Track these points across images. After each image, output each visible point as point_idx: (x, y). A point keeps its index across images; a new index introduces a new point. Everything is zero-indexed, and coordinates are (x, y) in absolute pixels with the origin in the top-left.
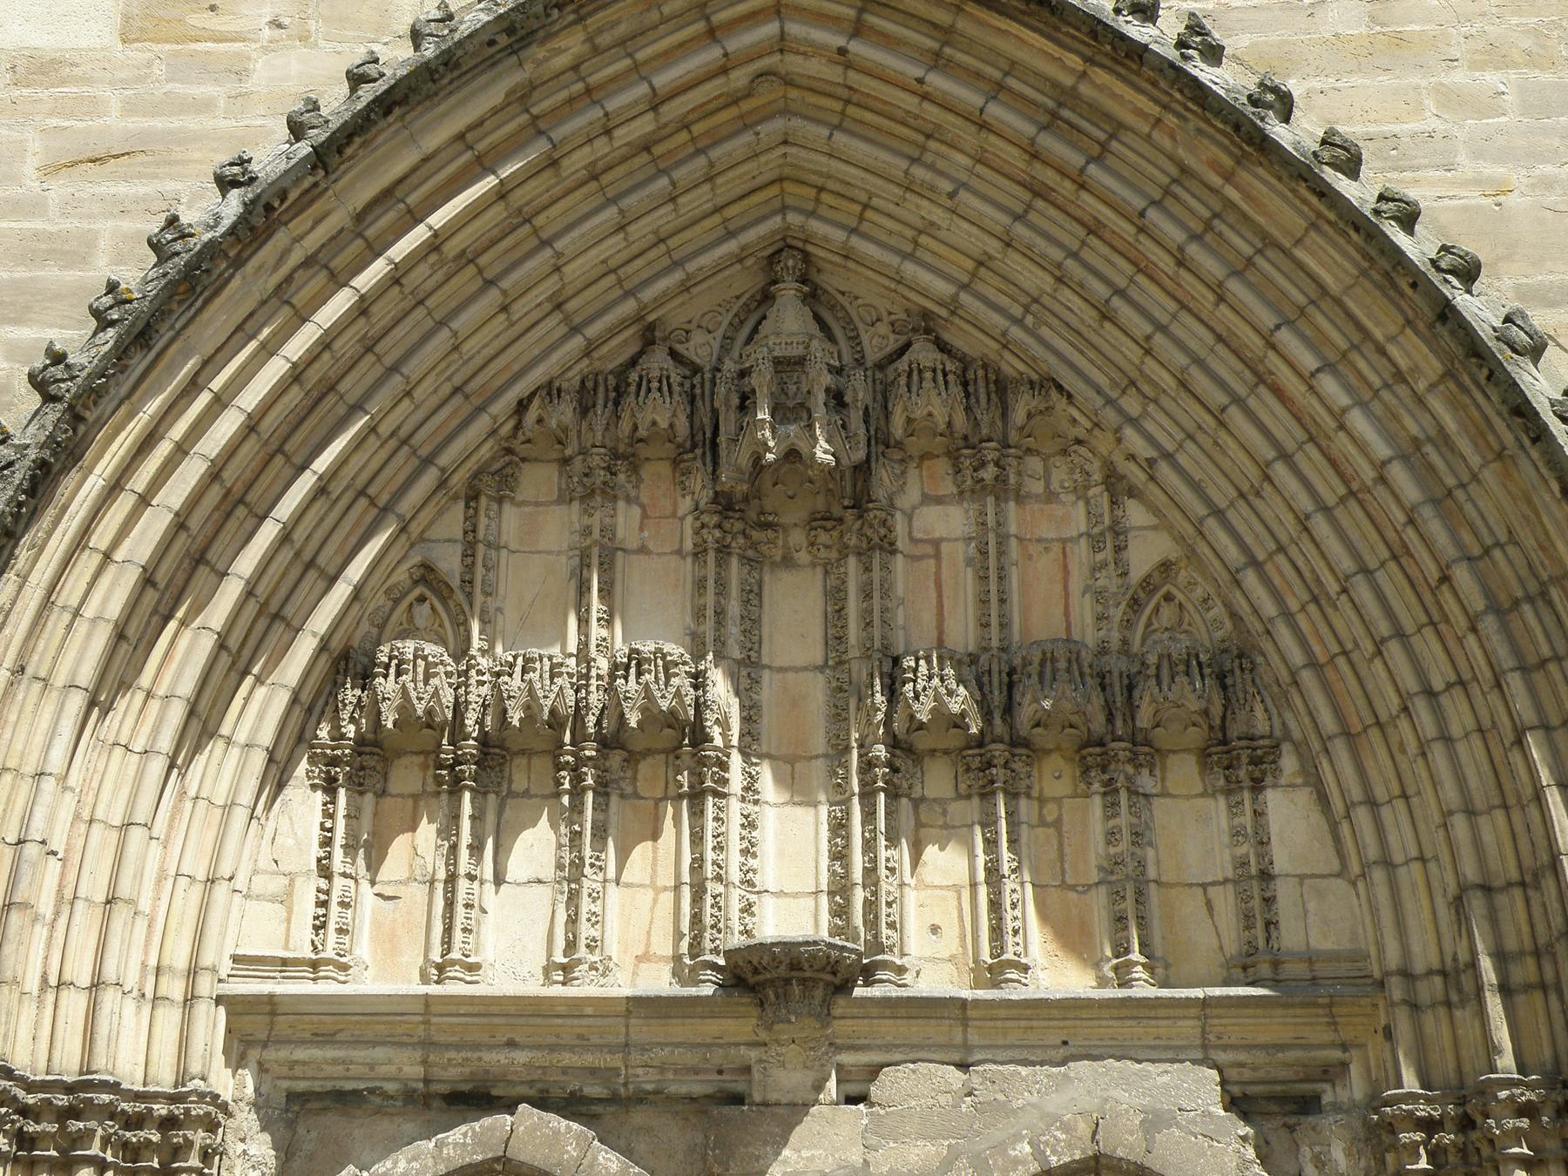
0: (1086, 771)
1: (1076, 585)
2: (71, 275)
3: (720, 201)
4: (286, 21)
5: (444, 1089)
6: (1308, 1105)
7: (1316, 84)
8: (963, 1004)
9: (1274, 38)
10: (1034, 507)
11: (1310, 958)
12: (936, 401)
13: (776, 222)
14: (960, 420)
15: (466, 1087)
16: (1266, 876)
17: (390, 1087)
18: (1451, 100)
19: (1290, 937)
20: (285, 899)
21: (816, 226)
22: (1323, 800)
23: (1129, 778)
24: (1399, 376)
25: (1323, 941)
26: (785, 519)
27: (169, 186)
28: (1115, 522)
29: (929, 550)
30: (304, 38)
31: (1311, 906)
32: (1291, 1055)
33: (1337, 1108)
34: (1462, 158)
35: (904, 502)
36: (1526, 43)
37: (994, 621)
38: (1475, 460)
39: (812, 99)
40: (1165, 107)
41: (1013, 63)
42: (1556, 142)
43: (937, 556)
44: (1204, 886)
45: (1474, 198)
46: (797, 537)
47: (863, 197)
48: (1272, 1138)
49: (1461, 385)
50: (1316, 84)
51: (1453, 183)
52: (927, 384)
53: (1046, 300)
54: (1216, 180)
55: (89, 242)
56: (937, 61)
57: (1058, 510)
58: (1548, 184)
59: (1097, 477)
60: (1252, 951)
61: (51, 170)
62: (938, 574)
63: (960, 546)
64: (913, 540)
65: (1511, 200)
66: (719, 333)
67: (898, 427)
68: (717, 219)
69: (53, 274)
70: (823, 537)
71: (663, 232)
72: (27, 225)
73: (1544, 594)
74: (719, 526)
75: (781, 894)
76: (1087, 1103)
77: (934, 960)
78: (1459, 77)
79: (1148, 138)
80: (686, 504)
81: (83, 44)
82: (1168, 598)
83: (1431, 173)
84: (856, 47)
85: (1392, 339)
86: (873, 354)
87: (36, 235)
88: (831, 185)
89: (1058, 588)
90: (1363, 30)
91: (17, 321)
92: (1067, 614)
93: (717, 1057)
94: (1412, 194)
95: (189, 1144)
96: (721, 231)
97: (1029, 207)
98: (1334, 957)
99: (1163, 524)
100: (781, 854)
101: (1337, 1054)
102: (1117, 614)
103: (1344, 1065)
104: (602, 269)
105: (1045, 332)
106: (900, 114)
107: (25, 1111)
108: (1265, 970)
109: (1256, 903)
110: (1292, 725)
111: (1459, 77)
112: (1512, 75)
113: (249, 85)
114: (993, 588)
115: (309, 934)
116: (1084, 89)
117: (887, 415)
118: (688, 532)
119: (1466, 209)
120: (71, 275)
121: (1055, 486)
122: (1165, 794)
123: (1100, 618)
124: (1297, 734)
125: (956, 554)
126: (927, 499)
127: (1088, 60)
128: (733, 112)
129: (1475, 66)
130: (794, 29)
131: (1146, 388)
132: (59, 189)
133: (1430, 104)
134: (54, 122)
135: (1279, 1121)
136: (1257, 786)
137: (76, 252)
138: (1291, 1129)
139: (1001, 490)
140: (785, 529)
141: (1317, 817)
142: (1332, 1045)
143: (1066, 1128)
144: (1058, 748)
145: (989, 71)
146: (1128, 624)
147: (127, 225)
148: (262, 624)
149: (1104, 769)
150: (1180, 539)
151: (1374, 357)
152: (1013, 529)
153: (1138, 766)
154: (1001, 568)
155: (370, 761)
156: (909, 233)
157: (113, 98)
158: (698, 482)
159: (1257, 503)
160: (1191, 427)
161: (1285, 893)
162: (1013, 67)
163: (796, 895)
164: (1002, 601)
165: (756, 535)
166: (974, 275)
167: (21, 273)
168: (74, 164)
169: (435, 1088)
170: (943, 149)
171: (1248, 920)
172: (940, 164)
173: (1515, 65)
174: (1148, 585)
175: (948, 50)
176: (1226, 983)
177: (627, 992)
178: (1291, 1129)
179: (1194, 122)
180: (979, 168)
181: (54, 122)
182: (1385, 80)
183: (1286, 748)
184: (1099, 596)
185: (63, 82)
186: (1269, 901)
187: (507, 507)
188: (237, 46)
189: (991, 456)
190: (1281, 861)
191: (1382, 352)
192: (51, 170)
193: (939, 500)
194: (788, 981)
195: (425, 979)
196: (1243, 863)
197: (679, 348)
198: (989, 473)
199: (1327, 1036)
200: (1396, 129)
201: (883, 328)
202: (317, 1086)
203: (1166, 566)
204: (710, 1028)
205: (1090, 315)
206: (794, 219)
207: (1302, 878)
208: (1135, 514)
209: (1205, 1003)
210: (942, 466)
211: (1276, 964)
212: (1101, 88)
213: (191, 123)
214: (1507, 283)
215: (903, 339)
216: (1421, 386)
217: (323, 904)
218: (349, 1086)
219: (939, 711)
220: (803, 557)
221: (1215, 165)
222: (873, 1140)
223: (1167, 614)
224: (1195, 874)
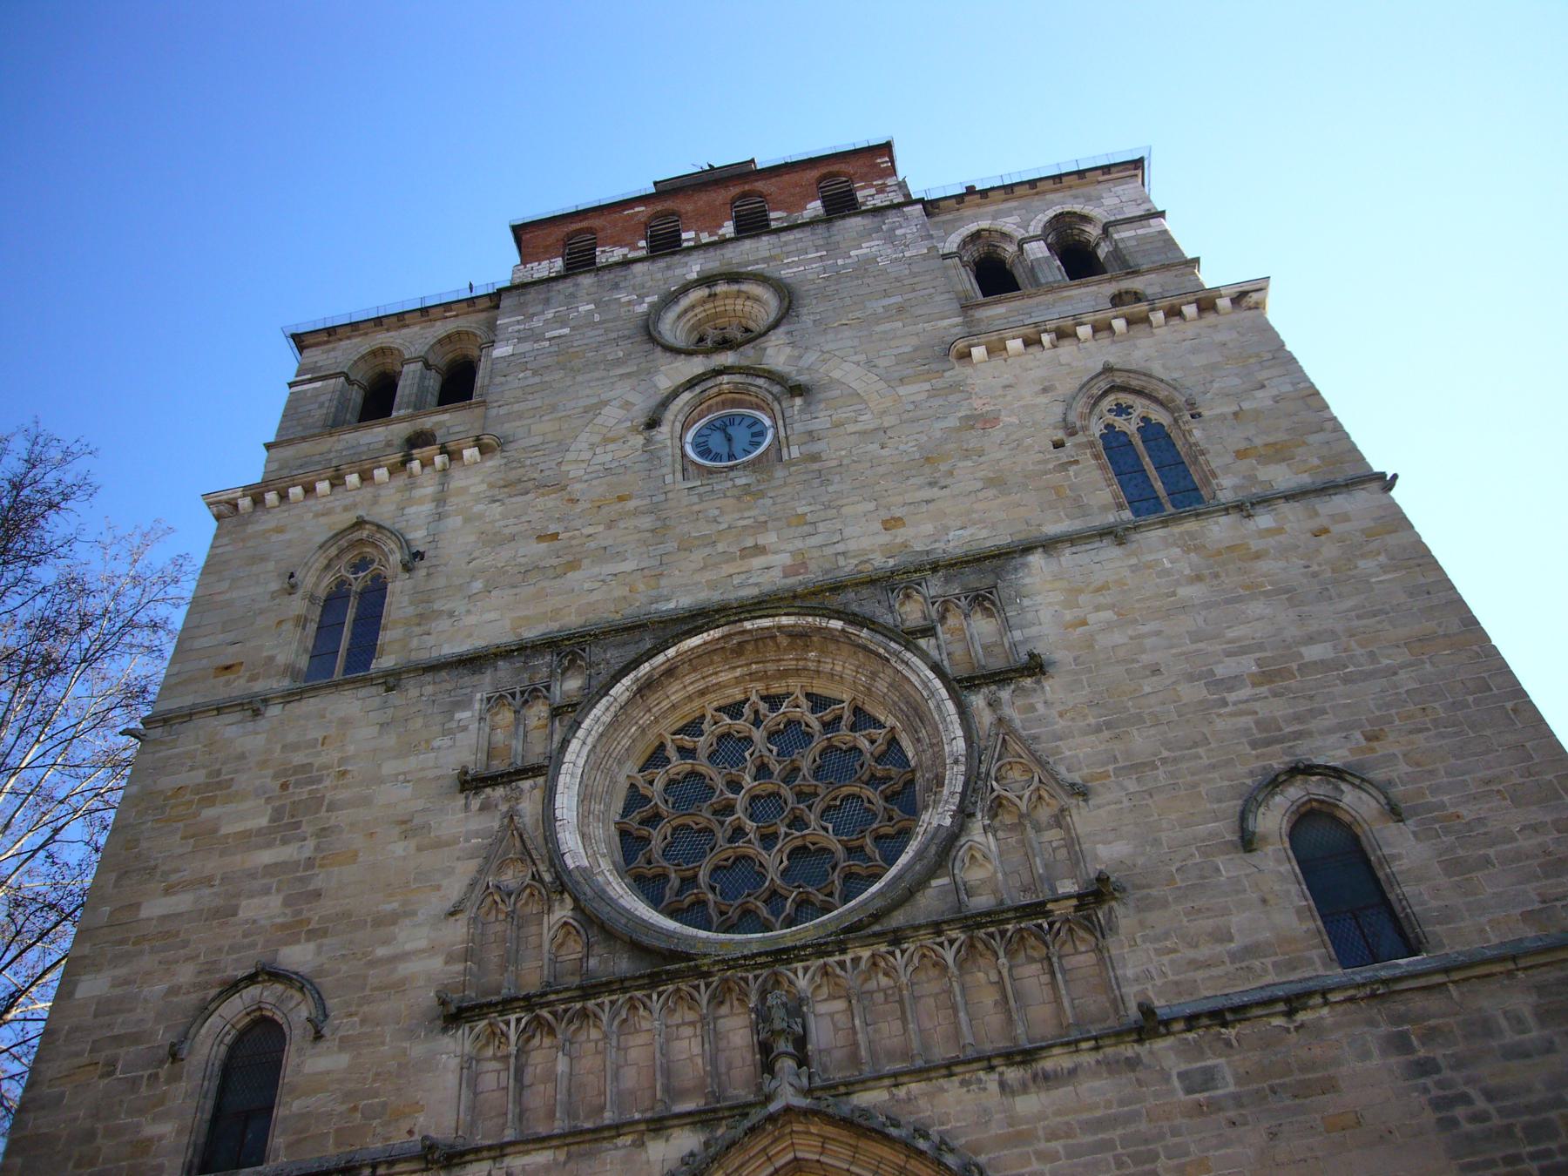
50: (992, 1155)
111: (1043, 1145)
129: (1048, 1140)
182: (1015, 1150)
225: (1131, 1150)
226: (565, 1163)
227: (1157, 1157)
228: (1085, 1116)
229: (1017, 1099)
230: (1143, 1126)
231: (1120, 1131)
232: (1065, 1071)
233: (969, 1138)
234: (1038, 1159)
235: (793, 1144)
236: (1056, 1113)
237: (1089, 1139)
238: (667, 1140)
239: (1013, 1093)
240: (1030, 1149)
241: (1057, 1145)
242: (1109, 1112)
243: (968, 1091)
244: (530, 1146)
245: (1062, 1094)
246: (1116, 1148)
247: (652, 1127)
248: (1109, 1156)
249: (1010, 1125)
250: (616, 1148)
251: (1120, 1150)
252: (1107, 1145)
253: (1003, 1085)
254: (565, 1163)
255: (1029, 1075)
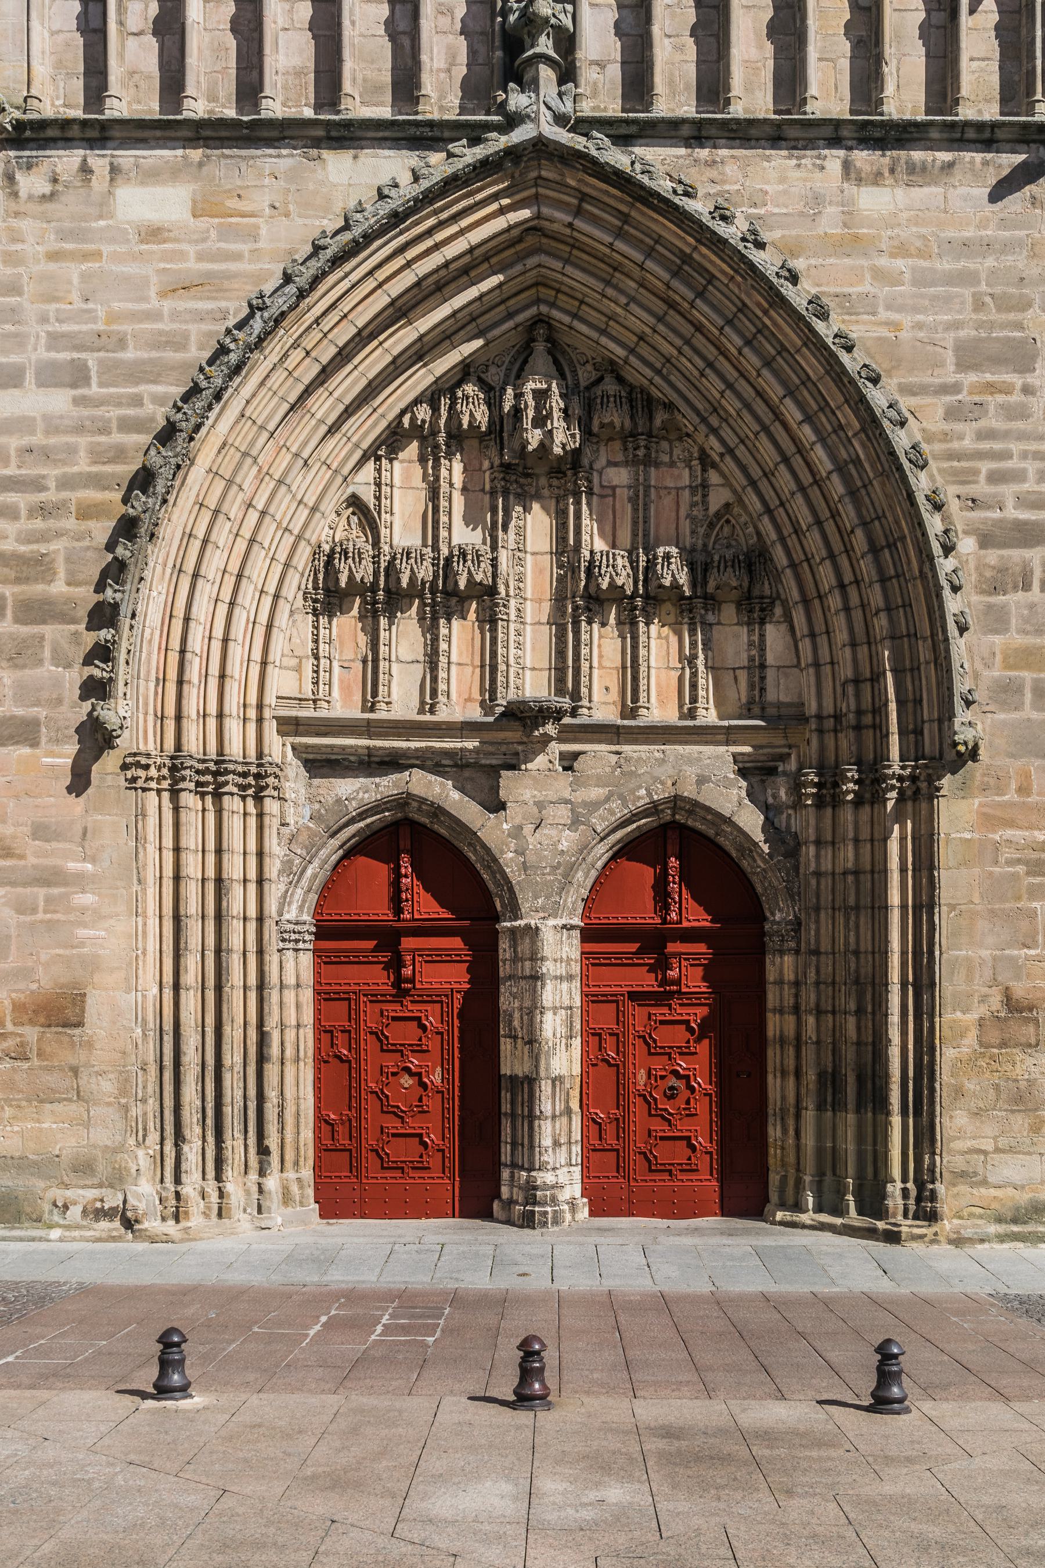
0: (682, 612)
1: (683, 513)
2: (179, 356)
3: (504, 296)
4: (277, 205)
5: (377, 759)
6: (772, 771)
7: (813, 262)
8: (618, 727)
9: (794, 233)
10: (664, 469)
11: (779, 705)
12: (616, 415)
13: (533, 311)
14: (628, 423)
15: (387, 759)
16: (763, 666)
17: (352, 758)
18: (880, 275)
19: (771, 696)
20: (298, 669)
21: (556, 314)
22: (792, 629)
23: (702, 616)
24: (841, 427)
25: (783, 698)
26: (537, 471)
27: (223, 304)
28: (704, 480)
29: (610, 492)
30: (287, 215)
31: (782, 681)
32: (766, 751)
33: (785, 773)
34: (881, 310)
35: (597, 466)
36: (919, 244)
37: (641, 520)
38: (871, 475)
39: (554, 244)
40: (736, 271)
41: (660, 236)
42: (927, 302)
43: (614, 495)
44: (734, 669)
45: (884, 332)
46: (543, 481)
47: (580, 296)
48: (755, 785)
49: (867, 436)
50: (813, 262)
51: (875, 323)
52: (611, 405)
53: (673, 360)
54: (760, 313)
55: (186, 336)
56: (619, 234)
57: (676, 472)
58: (919, 326)
59: (696, 455)
60: (751, 702)
61: (163, 294)
62: (614, 506)
63: (626, 490)
64: (602, 486)
65: (904, 335)
66: (504, 368)
67: (595, 428)
68: (502, 307)
69: (171, 356)
70: (555, 482)
71: (475, 314)
72: (155, 326)
73: (895, 544)
74: (504, 479)
75: (533, 669)
76: (671, 772)
77: (605, 703)
78: (883, 262)
79: (727, 286)
80: (486, 464)
81: (174, 218)
82: (728, 521)
83: (865, 317)
84: (578, 223)
85: (839, 408)
86: (583, 383)
87: (161, 333)
88: (564, 288)
89: (674, 514)
90: (839, 231)
91: (155, 382)
92: (677, 528)
93: (504, 748)
94: (853, 335)
95: (268, 786)
96: (505, 313)
97: (666, 313)
98: (789, 705)
99: (727, 483)
100: (533, 649)
101: (787, 750)
102: (701, 531)
103: (789, 755)
104: (443, 336)
105: (672, 378)
106: (600, 255)
107: (198, 772)
108: (756, 710)
109: (756, 679)
110: (781, 591)
111: (883, 262)
112: (910, 261)
113: (261, 245)
114: (641, 515)
115: (311, 686)
116: (695, 256)
117: (591, 419)
118: (487, 480)
119: (879, 339)
120: (179, 356)
121: (675, 458)
122: (719, 623)
123: (693, 532)
124: (783, 597)
125: (623, 494)
126: (611, 464)
127: (698, 241)
128: (512, 251)
129: (893, 255)
130: (541, 190)
131: (722, 413)
132: (167, 305)
133: (868, 276)
134: (162, 265)
135: (758, 778)
136: (762, 622)
137: (179, 343)
138: (763, 781)
139: (648, 462)
140: (538, 476)
141: (789, 638)
142: (784, 746)
143: (662, 783)
144: (669, 599)
145: (647, 240)
146: (707, 536)
147: (205, 327)
148: (280, 533)
149: (691, 611)
150: (734, 492)
151: (830, 415)
152: (653, 483)
153: (707, 610)
154: (645, 504)
155: (333, 600)
156: (604, 319)
157: (191, 249)
158: (493, 452)
159: (773, 479)
160: (743, 435)
161: (770, 674)
162: (659, 240)
163: (541, 670)
164: (645, 522)
165: (522, 480)
166: (637, 344)
167: (154, 354)
168: (174, 291)
169: (373, 759)
170: (623, 277)
171: (751, 686)
172: (621, 285)
173: (911, 256)
174: (718, 515)
175: (626, 227)
176: (740, 718)
177: (461, 719)
178: (763, 781)
179: (750, 281)
180: (641, 290)
181: (162, 265)
182: (847, 261)
183: (778, 603)
184: (693, 519)
185: (165, 242)
186: (763, 678)
187: (396, 463)
188: (253, 220)
189: (642, 443)
190: (770, 659)
191: (834, 413)
192: (163, 294)
193: (616, 464)
194: (536, 717)
195: (364, 710)
196: (751, 659)
197: (483, 376)
198: (641, 453)
199: (783, 742)
200: (850, 290)
201: (589, 367)
202: (318, 757)
203: (727, 505)
204: (501, 735)
205: (696, 373)
206: (544, 309)
207: (779, 667)
208: (714, 477)
209: (730, 727)
210: (617, 445)
211: (763, 709)
212: (704, 256)
213: (233, 266)
214: (895, 381)
215: (599, 374)
216: (850, 434)
217: (317, 672)
218: (334, 757)
219: (612, 584)
220: (546, 492)
221: (759, 305)
222: (575, 787)
223: (726, 529)
224: (730, 664)
225: (998, 290)
226: (201, 164)
227: (1029, 305)
228: (950, 234)
229: (863, 189)
230: (1018, 261)
231: (990, 262)
232: (938, 163)
233: (786, 232)
234: (873, 278)
235: (537, 196)
236: (916, 221)
237: (946, 265)
238: (355, 157)
239: (859, 181)
240: (863, 262)
241: (900, 264)
242: (983, 233)
243: (799, 166)
244: (147, 134)
245: (928, 194)
246: (979, 282)
247: (334, 134)
248: (967, 292)
249: (845, 225)
250: (279, 156)
251: (983, 287)
252: (968, 278)
253: (847, 165)
254: (201, 164)
255: (886, 161)
